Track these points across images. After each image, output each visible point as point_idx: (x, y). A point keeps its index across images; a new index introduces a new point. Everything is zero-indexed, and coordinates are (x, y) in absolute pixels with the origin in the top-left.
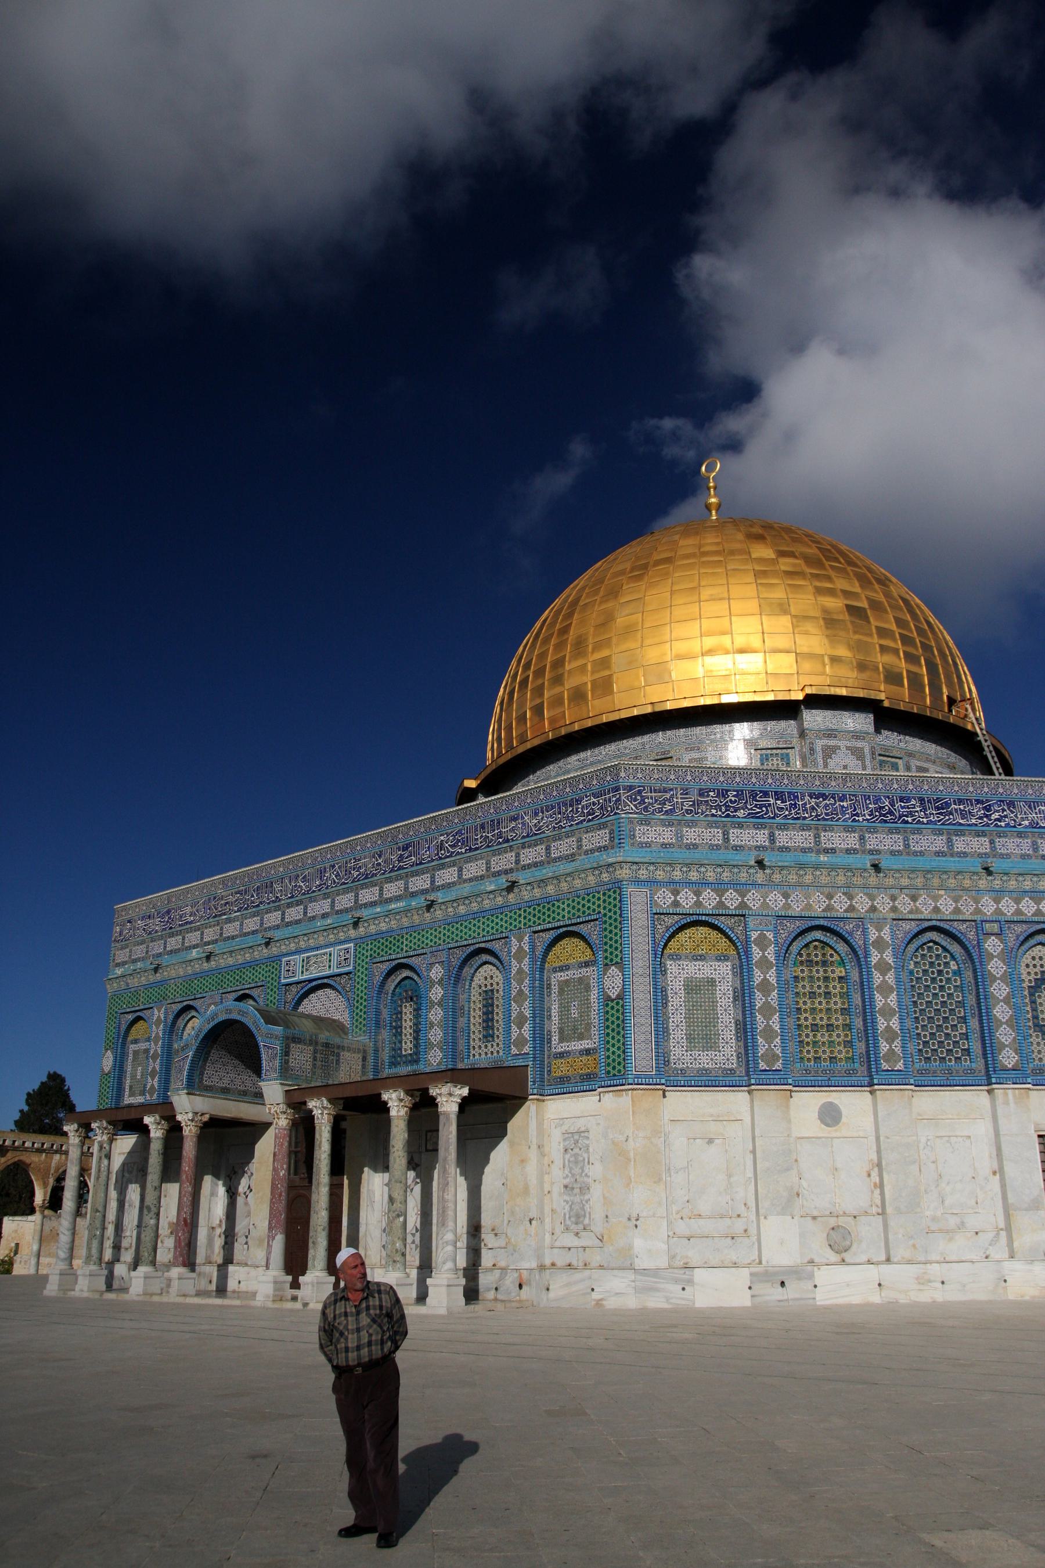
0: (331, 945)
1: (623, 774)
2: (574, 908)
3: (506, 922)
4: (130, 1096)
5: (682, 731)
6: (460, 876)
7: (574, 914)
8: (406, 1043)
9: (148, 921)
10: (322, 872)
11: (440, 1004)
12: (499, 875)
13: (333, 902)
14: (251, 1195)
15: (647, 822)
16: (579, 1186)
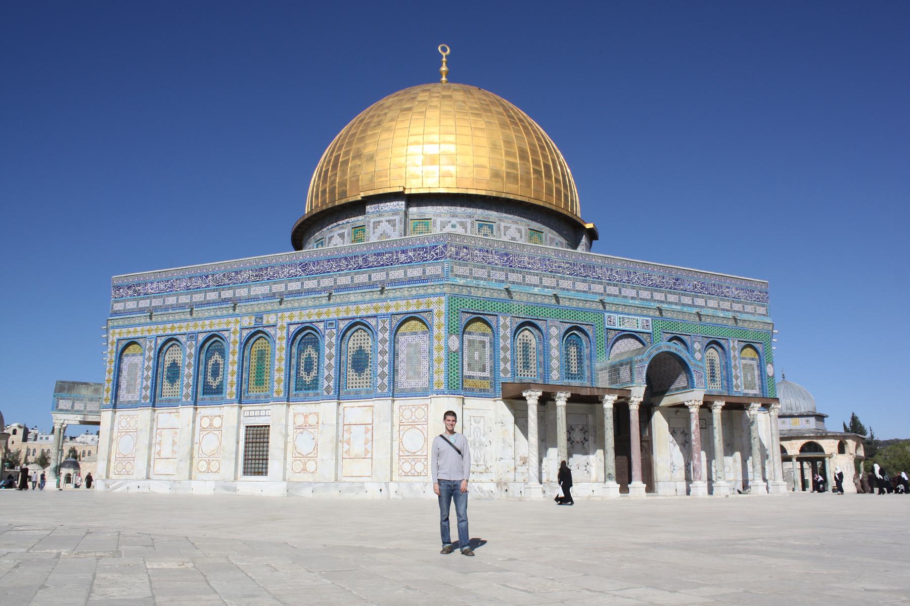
6: (706, 304)
9: (486, 254)
10: (629, 274)
14: (586, 444)
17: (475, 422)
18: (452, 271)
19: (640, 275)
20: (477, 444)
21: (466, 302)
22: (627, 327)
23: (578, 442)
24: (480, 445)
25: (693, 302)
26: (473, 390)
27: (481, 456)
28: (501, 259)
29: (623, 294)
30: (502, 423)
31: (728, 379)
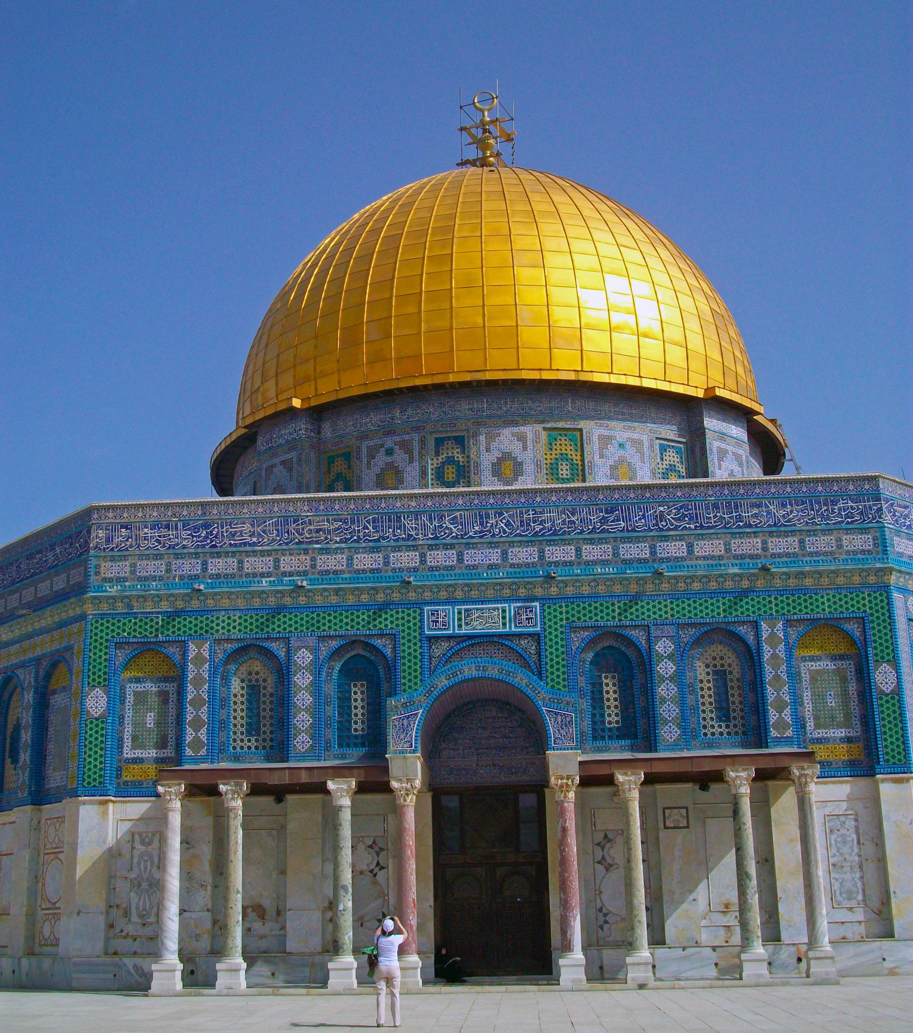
0: (505, 600)
1: (881, 486)
2: (835, 603)
3: (753, 606)
4: (134, 747)
5: (591, 405)
7: (836, 609)
8: (609, 715)
9: (164, 531)
10: (483, 519)
11: (671, 679)
12: (742, 558)
13: (504, 554)
14: (381, 875)
15: (898, 533)
16: (849, 864)
17: (143, 843)
18: (97, 573)
19: (511, 516)
20: (145, 885)
21: (124, 624)
22: (478, 627)
23: (361, 873)
24: (149, 885)
25: (653, 553)
26: (141, 783)
27: (151, 908)
28: (193, 536)
29: (468, 559)
30: (187, 843)
31: (758, 708)
